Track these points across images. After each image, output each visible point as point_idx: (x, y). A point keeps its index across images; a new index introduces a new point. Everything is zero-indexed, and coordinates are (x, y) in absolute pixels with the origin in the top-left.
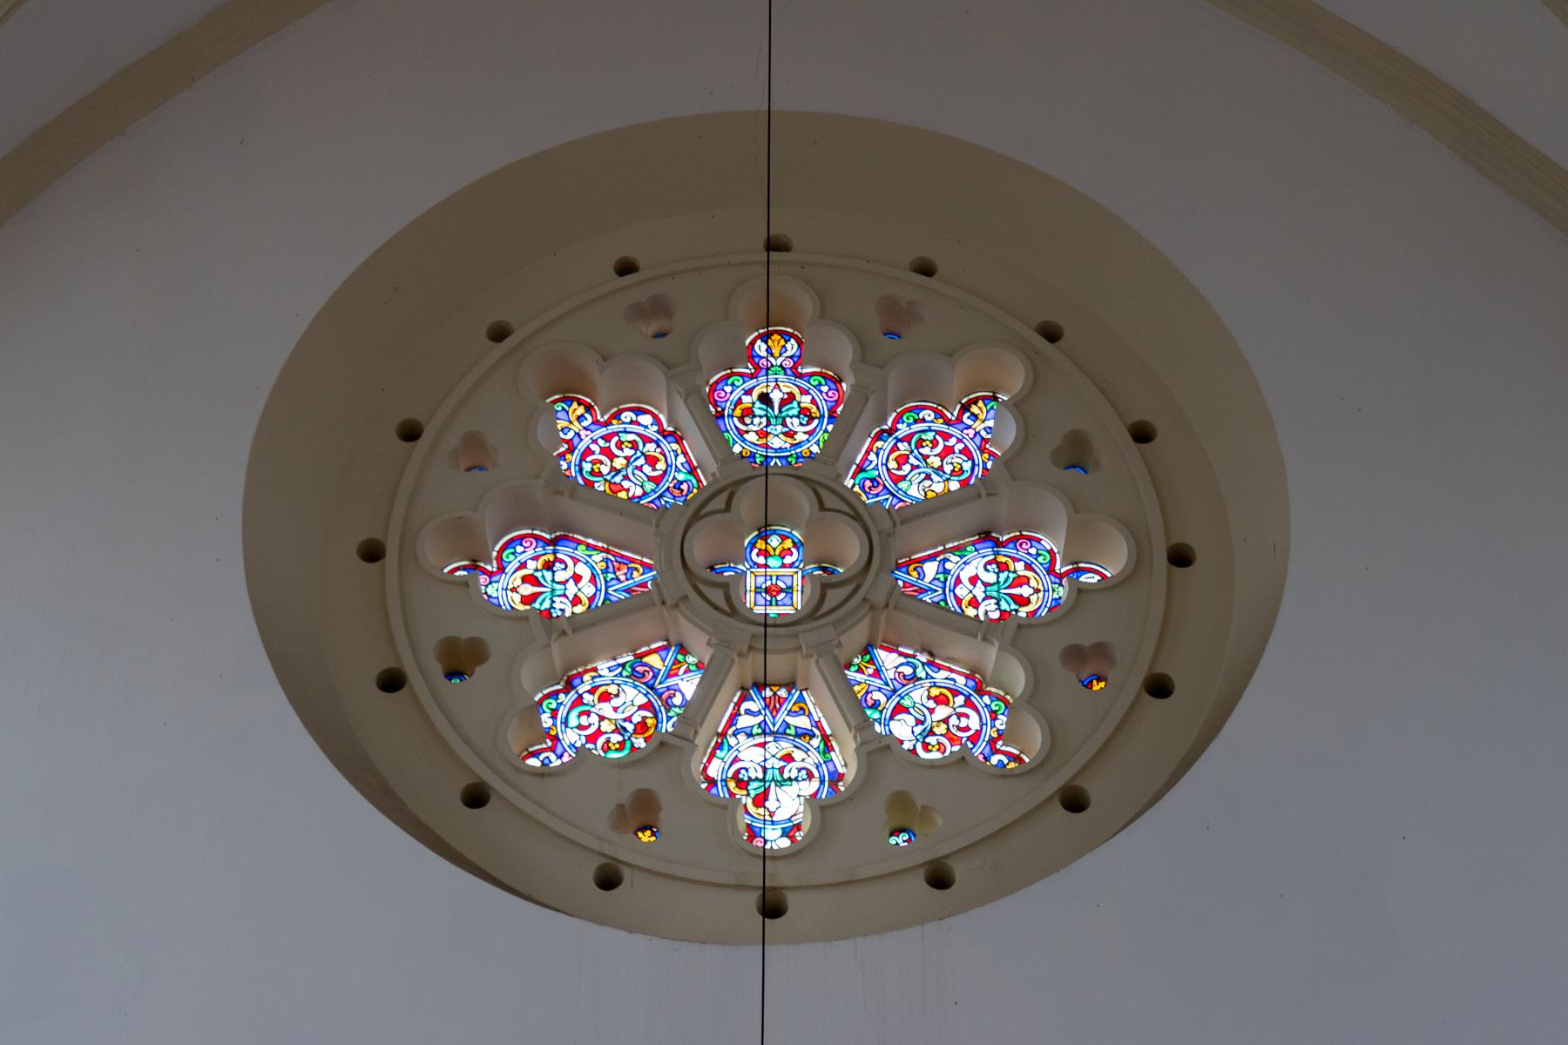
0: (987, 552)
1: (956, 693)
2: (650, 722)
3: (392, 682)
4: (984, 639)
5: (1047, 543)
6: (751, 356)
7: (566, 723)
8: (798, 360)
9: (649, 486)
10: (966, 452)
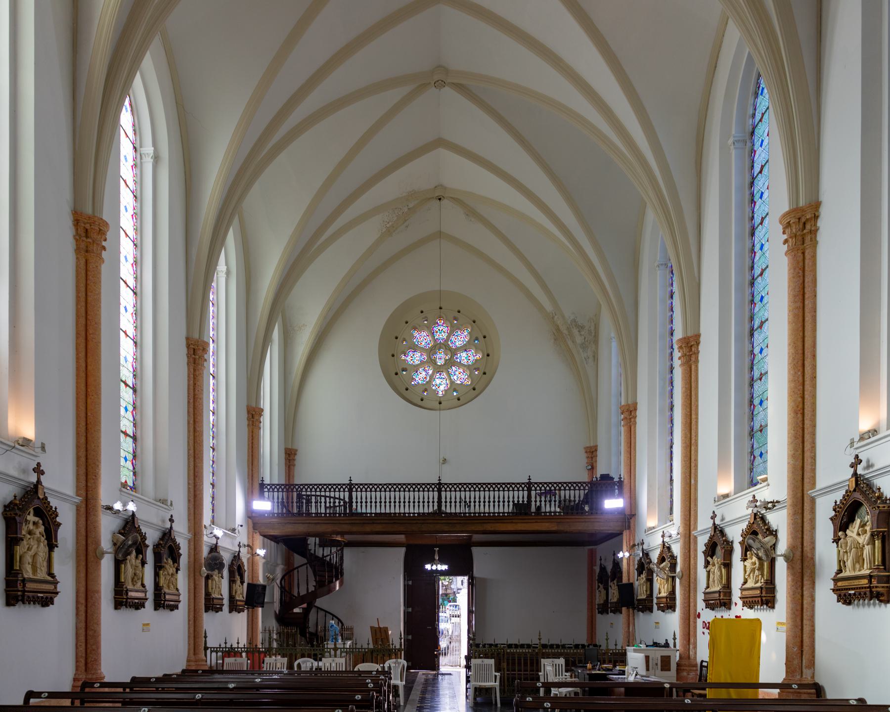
3: (396, 374)
6: (437, 323)
8: (443, 324)
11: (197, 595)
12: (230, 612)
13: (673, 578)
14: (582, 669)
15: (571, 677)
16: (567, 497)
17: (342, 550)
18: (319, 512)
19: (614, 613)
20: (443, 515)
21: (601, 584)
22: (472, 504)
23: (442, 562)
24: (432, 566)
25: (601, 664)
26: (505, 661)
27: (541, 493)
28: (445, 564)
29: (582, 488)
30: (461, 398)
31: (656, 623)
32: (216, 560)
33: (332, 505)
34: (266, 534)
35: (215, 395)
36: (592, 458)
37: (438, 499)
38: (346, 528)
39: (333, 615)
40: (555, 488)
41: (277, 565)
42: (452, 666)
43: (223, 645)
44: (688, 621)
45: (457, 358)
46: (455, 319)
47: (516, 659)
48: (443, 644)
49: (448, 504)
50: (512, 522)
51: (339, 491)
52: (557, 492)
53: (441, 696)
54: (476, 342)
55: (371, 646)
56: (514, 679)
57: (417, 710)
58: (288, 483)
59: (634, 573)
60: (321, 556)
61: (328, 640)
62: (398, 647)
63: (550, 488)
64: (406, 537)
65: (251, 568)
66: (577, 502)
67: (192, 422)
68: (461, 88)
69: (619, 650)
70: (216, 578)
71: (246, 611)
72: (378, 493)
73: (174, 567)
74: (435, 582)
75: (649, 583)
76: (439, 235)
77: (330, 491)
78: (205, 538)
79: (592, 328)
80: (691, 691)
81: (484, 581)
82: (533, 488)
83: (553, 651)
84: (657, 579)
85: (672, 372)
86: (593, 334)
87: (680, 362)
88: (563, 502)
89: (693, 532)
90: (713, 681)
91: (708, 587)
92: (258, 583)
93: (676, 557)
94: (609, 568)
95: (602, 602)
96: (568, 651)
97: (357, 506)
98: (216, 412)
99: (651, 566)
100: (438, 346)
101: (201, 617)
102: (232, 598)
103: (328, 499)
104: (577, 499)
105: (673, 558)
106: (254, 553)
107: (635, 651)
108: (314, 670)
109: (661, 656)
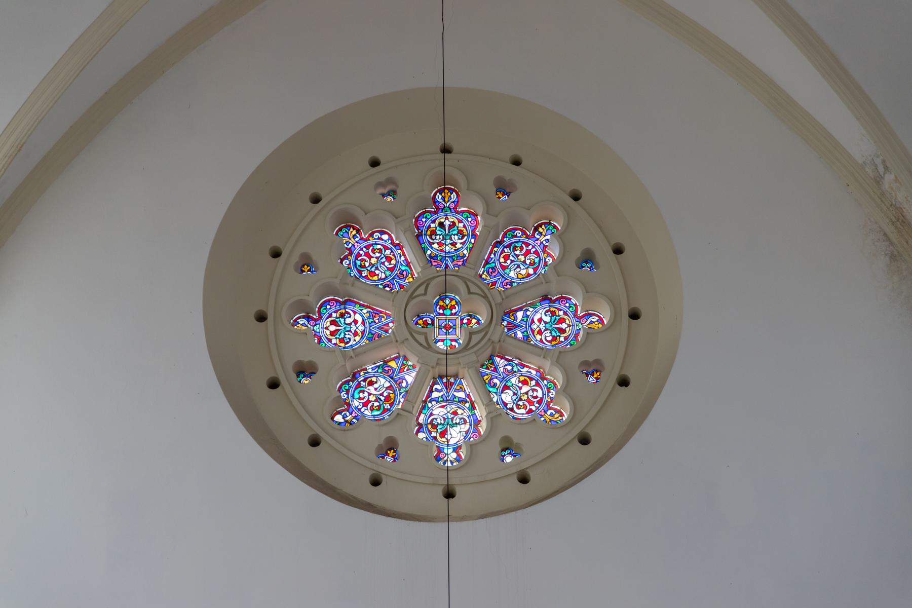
0: (546, 305)
1: (532, 379)
2: (392, 396)
4: (544, 357)
7: (353, 396)
8: (457, 203)
9: (388, 273)
10: (536, 252)
30: (533, 475)
45: (512, 327)
46: (503, 188)
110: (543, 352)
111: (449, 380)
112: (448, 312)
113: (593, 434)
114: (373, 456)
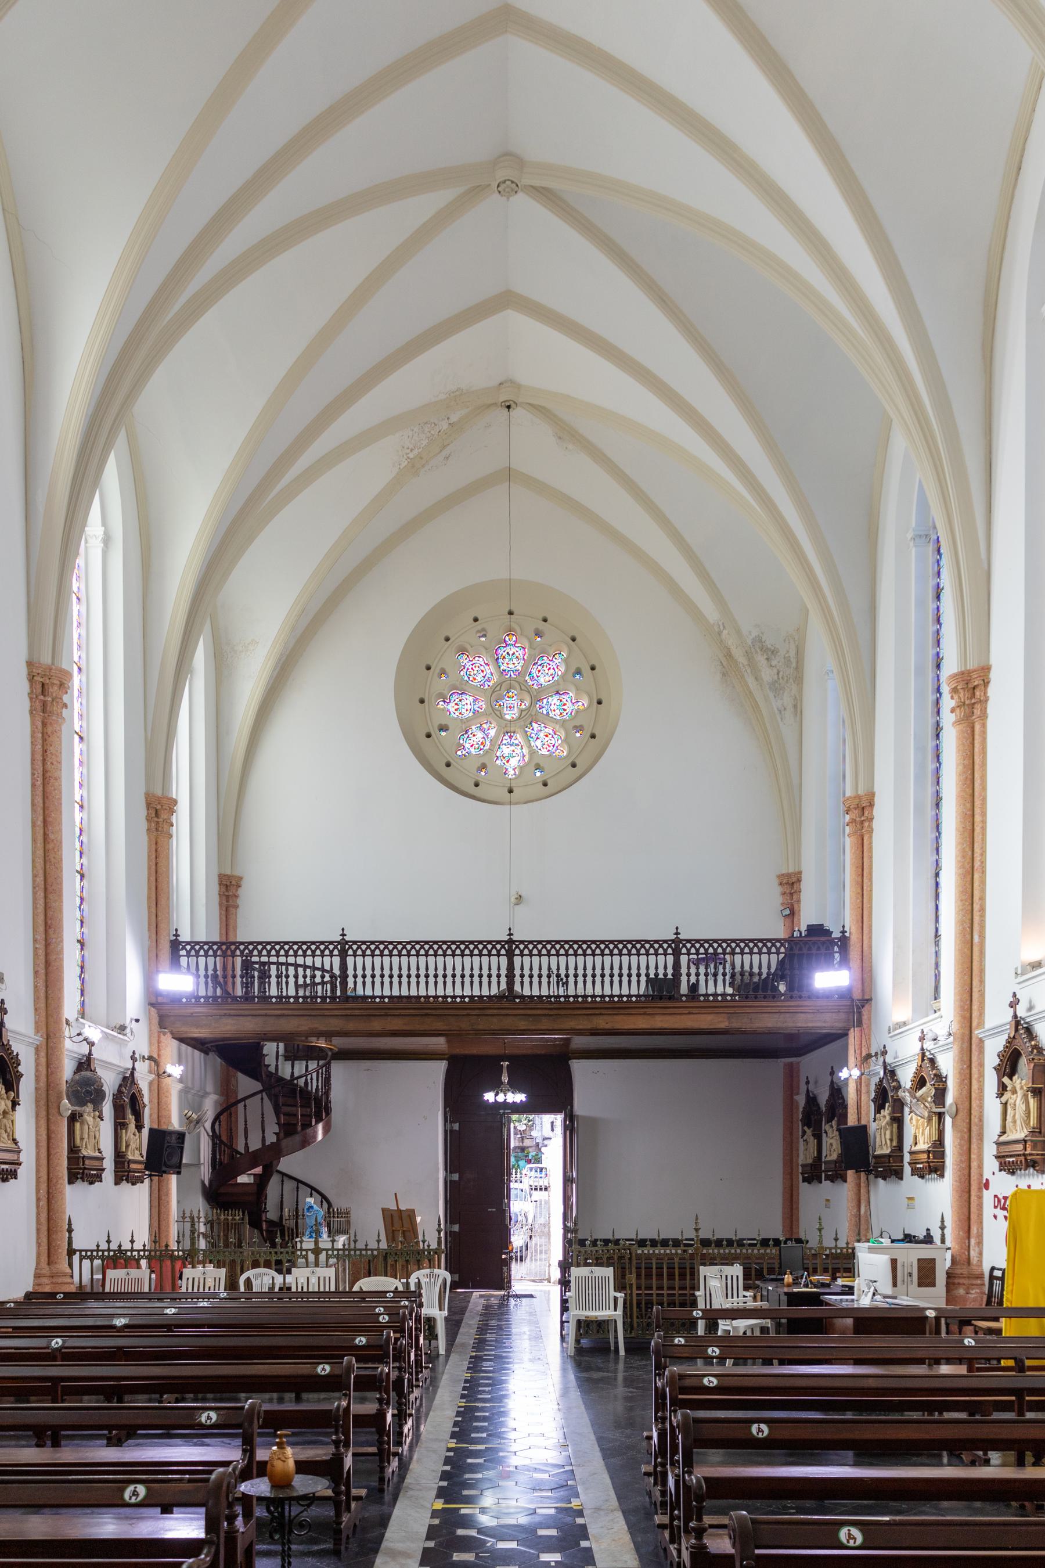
0: (558, 696)
3: (429, 736)
5: (571, 694)
6: (505, 641)
8: (516, 642)
11: (53, 1152)
12: (117, 1183)
13: (940, 1116)
14: (774, 1284)
15: (755, 1298)
16: (747, 968)
17: (328, 1066)
18: (284, 994)
19: (832, 1181)
20: (518, 1000)
21: (809, 1128)
22: (571, 979)
23: (515, 1087)
24: (496, 1095)
25: (808, 1275)
26: (634, 1270)
27: (698, 959)
28: (521, 1091)
29: (773, 950)
30: (549, 782)
31: (909, 1198)
32: (90, 1085)
33: (308, 981)
34: (185, 1036)
35: (85, 772)
36: (791, 894)
37: (507, 970)
38: (335, 1024)
39: (313, 1188)
40: (724, 950)
41: (206, 1094)
42: (534, 1281)
43: (104, 1246)
44: (967, 1195)
45: (541, 707)
46: (538, 633)
47: (654, 1267)
48: (517, 1240)
49: (527, 979)
50: (645, 1014)
51: (322, 955)
52: (727, 957)
53: (514, 1337)
54: (578, 676)
55: (384, 1245)
56: (649, 1304)
57: (470, 1363)
58: (224, 940)
59: (869, 1106)
60: (288, 1077)
61: (303, 1234)
62: (434, 1246)
63: (715, 950)
64: (448, 1042)
65: (156, 1101)
66: (764, 976)
67: (40, 823)
68: (546, 195)
69: (842, 1249)
70: (89, 1119)
71: (147, 1181)
72: (395, 959)
73: (8, 1098)
74: (501, 1124)
75: (895, 1126)
76: (508, 475)
77: (305, 955)
78: (68, 1044)
79: (792, 654)
80: (974, 1322)
81: (593, 1122)
82: (684, 951)
83: (722, 1251)
84: (911, 1119)
85: (938, 736)
86: (794, 665)
87: (952, 717)
88: (738, 977)
89: (976, 1032)
90: (1014, 1305)
91: (1004, 1132)
92: (171, 1128)
93: (946, 1077)
94: (823, 1098)
95: (810, 1161)
96: (750, 1251)
97: (355, 983)
98: (85, 805)
99: (900, 1093)
100: (506, 684)
101: (62, 1193)
102: (119, 1157)
103: (300, 970)
104: (765, 970)
105: (940, 1078)
106: (161, 1073)
107: (871, 1250)
108: (277, 1290)
109: (919, 1260)
110: (556, 721)
111: (510, 733)
112: (511, 699)
113: (578, 762)
114: (475, 770)
